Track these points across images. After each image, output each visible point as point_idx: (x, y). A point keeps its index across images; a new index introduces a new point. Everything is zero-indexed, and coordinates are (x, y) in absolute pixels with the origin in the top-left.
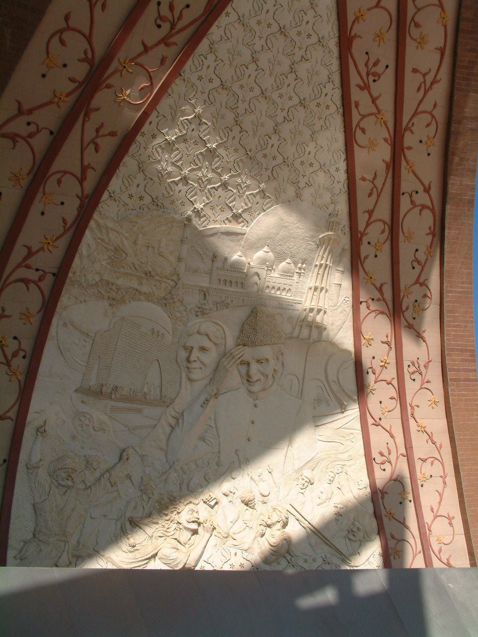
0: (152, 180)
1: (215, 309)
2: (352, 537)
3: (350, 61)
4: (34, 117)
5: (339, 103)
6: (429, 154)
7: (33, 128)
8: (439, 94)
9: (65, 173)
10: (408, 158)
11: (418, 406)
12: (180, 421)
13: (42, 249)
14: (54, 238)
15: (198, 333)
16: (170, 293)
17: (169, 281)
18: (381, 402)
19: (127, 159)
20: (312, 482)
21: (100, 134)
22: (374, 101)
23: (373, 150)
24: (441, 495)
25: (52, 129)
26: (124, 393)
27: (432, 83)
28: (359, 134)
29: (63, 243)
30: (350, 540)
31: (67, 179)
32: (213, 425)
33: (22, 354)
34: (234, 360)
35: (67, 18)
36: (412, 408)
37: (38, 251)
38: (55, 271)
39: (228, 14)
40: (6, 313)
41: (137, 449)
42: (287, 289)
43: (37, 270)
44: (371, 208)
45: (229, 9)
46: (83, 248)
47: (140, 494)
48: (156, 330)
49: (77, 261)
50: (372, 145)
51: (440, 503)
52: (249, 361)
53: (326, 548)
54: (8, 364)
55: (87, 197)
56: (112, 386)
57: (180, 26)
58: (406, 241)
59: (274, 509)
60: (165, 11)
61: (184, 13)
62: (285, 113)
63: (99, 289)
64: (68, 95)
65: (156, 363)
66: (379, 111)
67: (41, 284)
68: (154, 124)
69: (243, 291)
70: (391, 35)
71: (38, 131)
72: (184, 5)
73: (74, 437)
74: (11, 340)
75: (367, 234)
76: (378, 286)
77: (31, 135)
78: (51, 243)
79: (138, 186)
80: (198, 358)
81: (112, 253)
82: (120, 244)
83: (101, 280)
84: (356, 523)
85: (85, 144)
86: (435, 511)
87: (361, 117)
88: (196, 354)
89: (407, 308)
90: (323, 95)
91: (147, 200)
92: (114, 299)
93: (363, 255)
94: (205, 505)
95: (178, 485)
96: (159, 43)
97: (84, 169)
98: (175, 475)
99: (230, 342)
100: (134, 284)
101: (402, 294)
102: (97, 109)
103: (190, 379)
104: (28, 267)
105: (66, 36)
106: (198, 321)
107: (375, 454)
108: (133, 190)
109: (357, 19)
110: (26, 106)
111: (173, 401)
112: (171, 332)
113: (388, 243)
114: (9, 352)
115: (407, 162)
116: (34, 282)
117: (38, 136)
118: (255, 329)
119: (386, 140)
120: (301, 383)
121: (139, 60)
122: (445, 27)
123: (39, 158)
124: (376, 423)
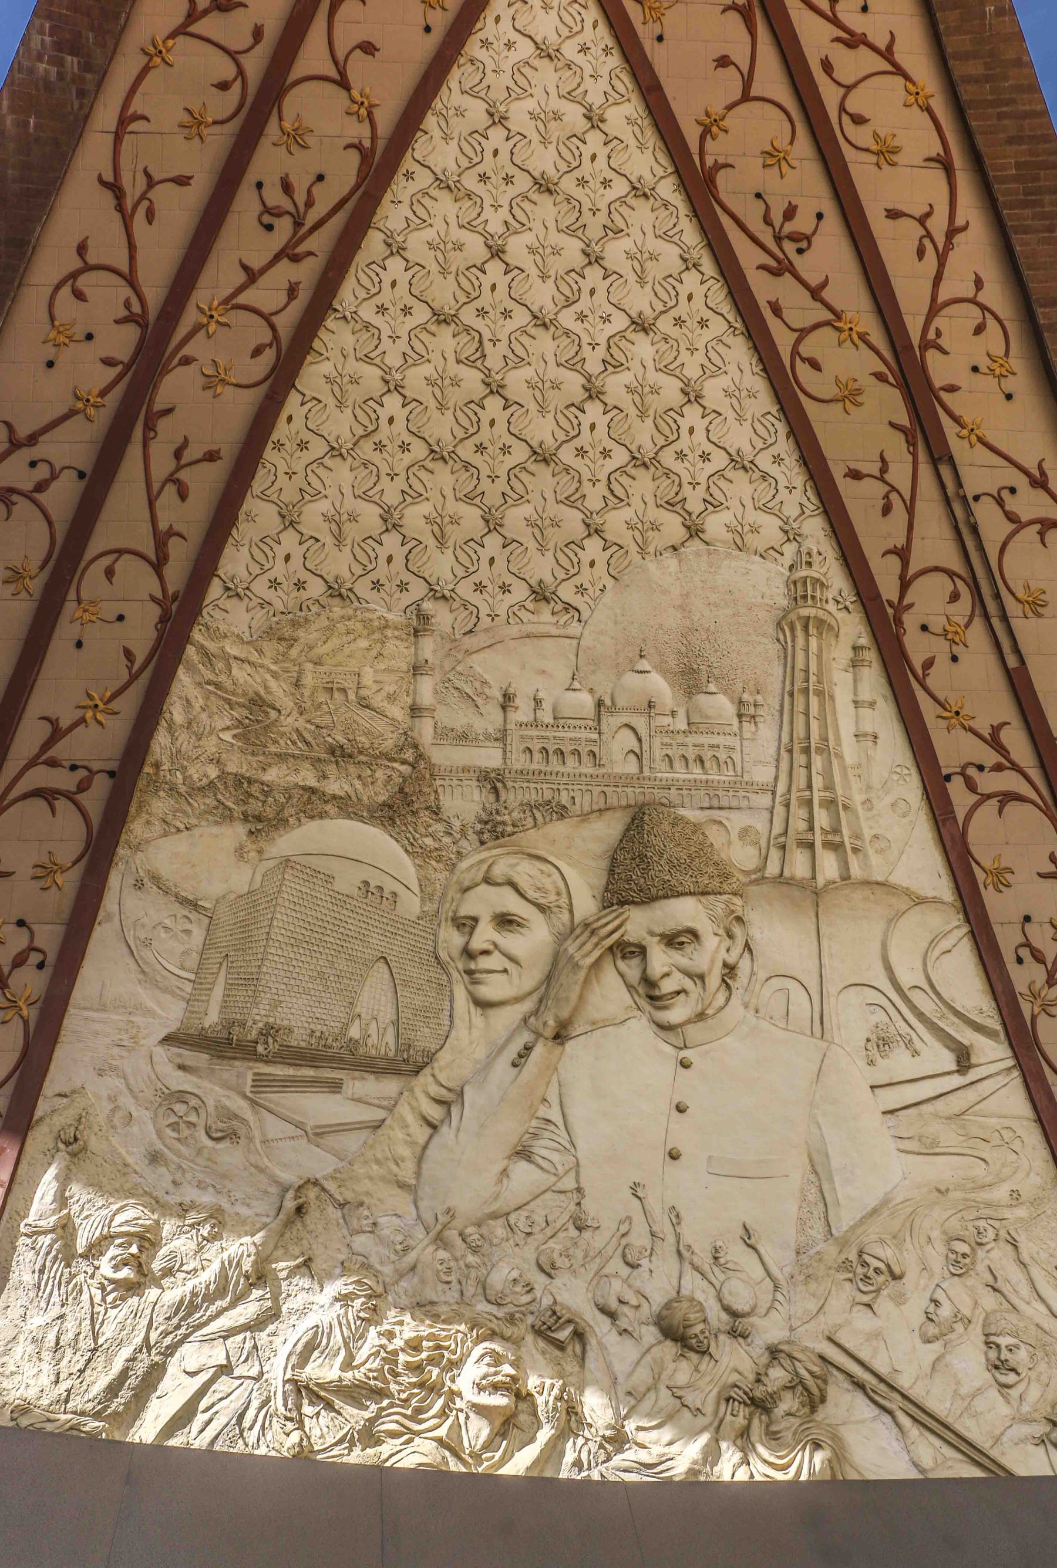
0: (317, 540)
1: (530, 822)
3: (725, 221)
4: (43, 449)
5: (726, 308)
6: (1009, 397)
8: (975, 255)
9: (120, 552)
10: (957, 412)
12: (455, 1111)
13: (83, 720)
14: (108, 694)
15: (488, 880)
16: (401, 790)
17: (396, 765)
19: (250, 504)
20: (897, 1270)
21: (183, 462)
22: (816, 293)
23: (859, 405)
26: (295, 1044)
27: (952, 232)
28: (803, 371)
29: (129, 704)
31: (126, 566)
33: (35, 958)
34: (594, 939)
35: (82, 249)
38: (113, 765)
39: (409, 176)
41: (331, 1186)
43: (74, 768)
44: (901, 542)
45: (408, 163)
46: (176, 711)
48: (373, 884)
49: (161, 739)
50: (849, 396)
52: (644, 943)
55: (175, 597)
56: (260, 1025)
57: (312, 217)
58: (1030, 614)
59: (774, 1352)
60: (275, 197)
61: (315, 190)
63: (220, 797)
64: (103, 394)
65: (381, 965)
66: (838, 316)
67: (83, 798)
68: (298, 422)
70: (803, 147)
71: (54, 476)
72: (313, 178)
73: (155, 1158)
74: (12, 928)
75: (910, 606)
76: (986, 732)
77: (41, 487)
78: (101, 706)
79: (287, 558)
80: (496, 945)
81: (245, 713)
82: (262, 692)
83: (223, 775)
85: (156, 487)
87: (796, 335)
88: (485, 935)
90: (683, 298)
91: (316, 588)
92: (259, 819)
94: (542, 1344)
95: (455, 1286)
96: (277, 258)
97: (161, 540)
98: (442, 1254)
99: (586, 905)
100: (308, 777)
102: (169, 411)
103: (483, 1005)
104: (53, 763)
105: (82, 282)
106: (484, 855)
108: (279, 570)
110: (23, 431)
111: (430, 1058)
112: (416, 889)
115: (957, 420)
116: (68, 796)
118: (642, 857)
119: (880, 377)
121: (241, 299)
122: (929, 110)
123: (61, 530)
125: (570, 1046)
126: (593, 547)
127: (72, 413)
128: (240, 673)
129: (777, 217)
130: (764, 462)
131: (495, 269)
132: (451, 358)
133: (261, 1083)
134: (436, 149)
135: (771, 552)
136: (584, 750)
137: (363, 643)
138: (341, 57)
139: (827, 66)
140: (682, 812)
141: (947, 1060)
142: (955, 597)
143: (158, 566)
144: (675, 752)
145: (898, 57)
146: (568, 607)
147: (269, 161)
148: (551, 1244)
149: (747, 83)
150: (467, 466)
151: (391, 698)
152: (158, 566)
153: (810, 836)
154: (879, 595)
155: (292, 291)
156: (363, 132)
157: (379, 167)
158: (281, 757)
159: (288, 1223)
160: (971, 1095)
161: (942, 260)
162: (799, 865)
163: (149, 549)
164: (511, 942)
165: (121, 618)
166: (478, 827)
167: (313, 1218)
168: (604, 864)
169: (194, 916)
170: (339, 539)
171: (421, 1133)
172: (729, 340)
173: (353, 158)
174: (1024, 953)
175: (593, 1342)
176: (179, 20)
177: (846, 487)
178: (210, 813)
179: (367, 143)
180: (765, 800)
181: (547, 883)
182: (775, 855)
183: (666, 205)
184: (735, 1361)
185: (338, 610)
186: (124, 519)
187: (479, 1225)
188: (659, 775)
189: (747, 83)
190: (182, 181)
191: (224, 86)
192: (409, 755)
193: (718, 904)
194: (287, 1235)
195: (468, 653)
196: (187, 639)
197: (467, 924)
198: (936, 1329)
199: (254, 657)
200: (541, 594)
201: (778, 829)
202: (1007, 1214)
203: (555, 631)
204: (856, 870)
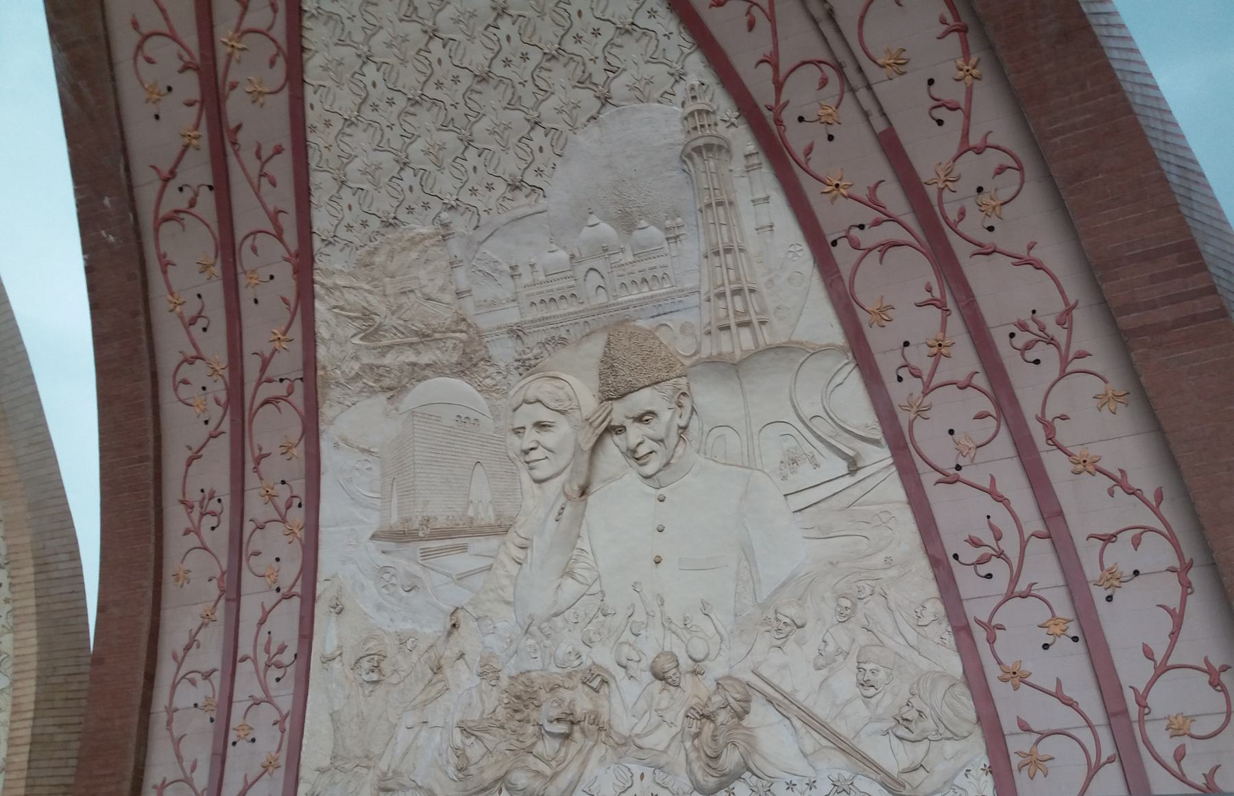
2: (902, 732)
7: (188, 194)
9: (254, 233)
13: (275, 350)
17: (458, 335)
18: (951, 432)
19: (316, 178)
24: (1178, 618)
25: (211, 183)
29: (296, 331)
30: (901, 739)
33: (296, 502)
36: (1049, 429)
40: (264, 452)
41: (470, 609)
42: (659, 274)
43: (281, 380)
46: (322, 331)
49: (321, 352)
51: (1174, 635)
67: (290, 398)
69: (581, 308)
71: (196, 195)
73: (379, 607)
77: (192, 204)
80: (538, 442)
81: (361, 322)
82: (365, 305)
84: (916, 702)
86: (1159, 657)
88: (531, 437)
91: (375, 224)
92: (390, 389)
95: (539, 659)
98: (531, 642)
103: (539, 482)
104: (270, 381)
106: (523, 382)
107: (952, 543)
108: (349, 218)
111: (513, 520)
117: (199, 199)
120: (744, 438)
124: (949, 479)
125: (591, 499)
133: (426, 554)
135: (666, 96)
136: (567, 294)
137: (414, 255)
140: (640, 323)
141: (842, 466)
143: (279, 236)
144: (627, 280)
148: (589, 627)
151: (442, 289)
152: (279, 236)
153: (726, 322)
154: (756, 106)
158: (390, 347)
159: (450, 634)
160: (856, 492)
162: (725, 344)
163: (269, 227)
164: (548, 438)
165: (272, 277)
166: (516, 364)
167: (463, 629)
168: (595, 372)
169: (370, 458)
171: (513, 569)
174: (904, 373)
178: (361, 391)
181: (561, 394)
182: (706, 341)
185: (391, 235)
187: (548, 620)
188: (620, 300)
192: (463, 326)
193: (667, 387)
194: (452, 640)
195: (480, 243)
196: (313, 282)
197: (518, 431)
198: (825, 662)
199: (356, 284)
200: (515, 187)
202: (882, 575)
203: (530, 211)
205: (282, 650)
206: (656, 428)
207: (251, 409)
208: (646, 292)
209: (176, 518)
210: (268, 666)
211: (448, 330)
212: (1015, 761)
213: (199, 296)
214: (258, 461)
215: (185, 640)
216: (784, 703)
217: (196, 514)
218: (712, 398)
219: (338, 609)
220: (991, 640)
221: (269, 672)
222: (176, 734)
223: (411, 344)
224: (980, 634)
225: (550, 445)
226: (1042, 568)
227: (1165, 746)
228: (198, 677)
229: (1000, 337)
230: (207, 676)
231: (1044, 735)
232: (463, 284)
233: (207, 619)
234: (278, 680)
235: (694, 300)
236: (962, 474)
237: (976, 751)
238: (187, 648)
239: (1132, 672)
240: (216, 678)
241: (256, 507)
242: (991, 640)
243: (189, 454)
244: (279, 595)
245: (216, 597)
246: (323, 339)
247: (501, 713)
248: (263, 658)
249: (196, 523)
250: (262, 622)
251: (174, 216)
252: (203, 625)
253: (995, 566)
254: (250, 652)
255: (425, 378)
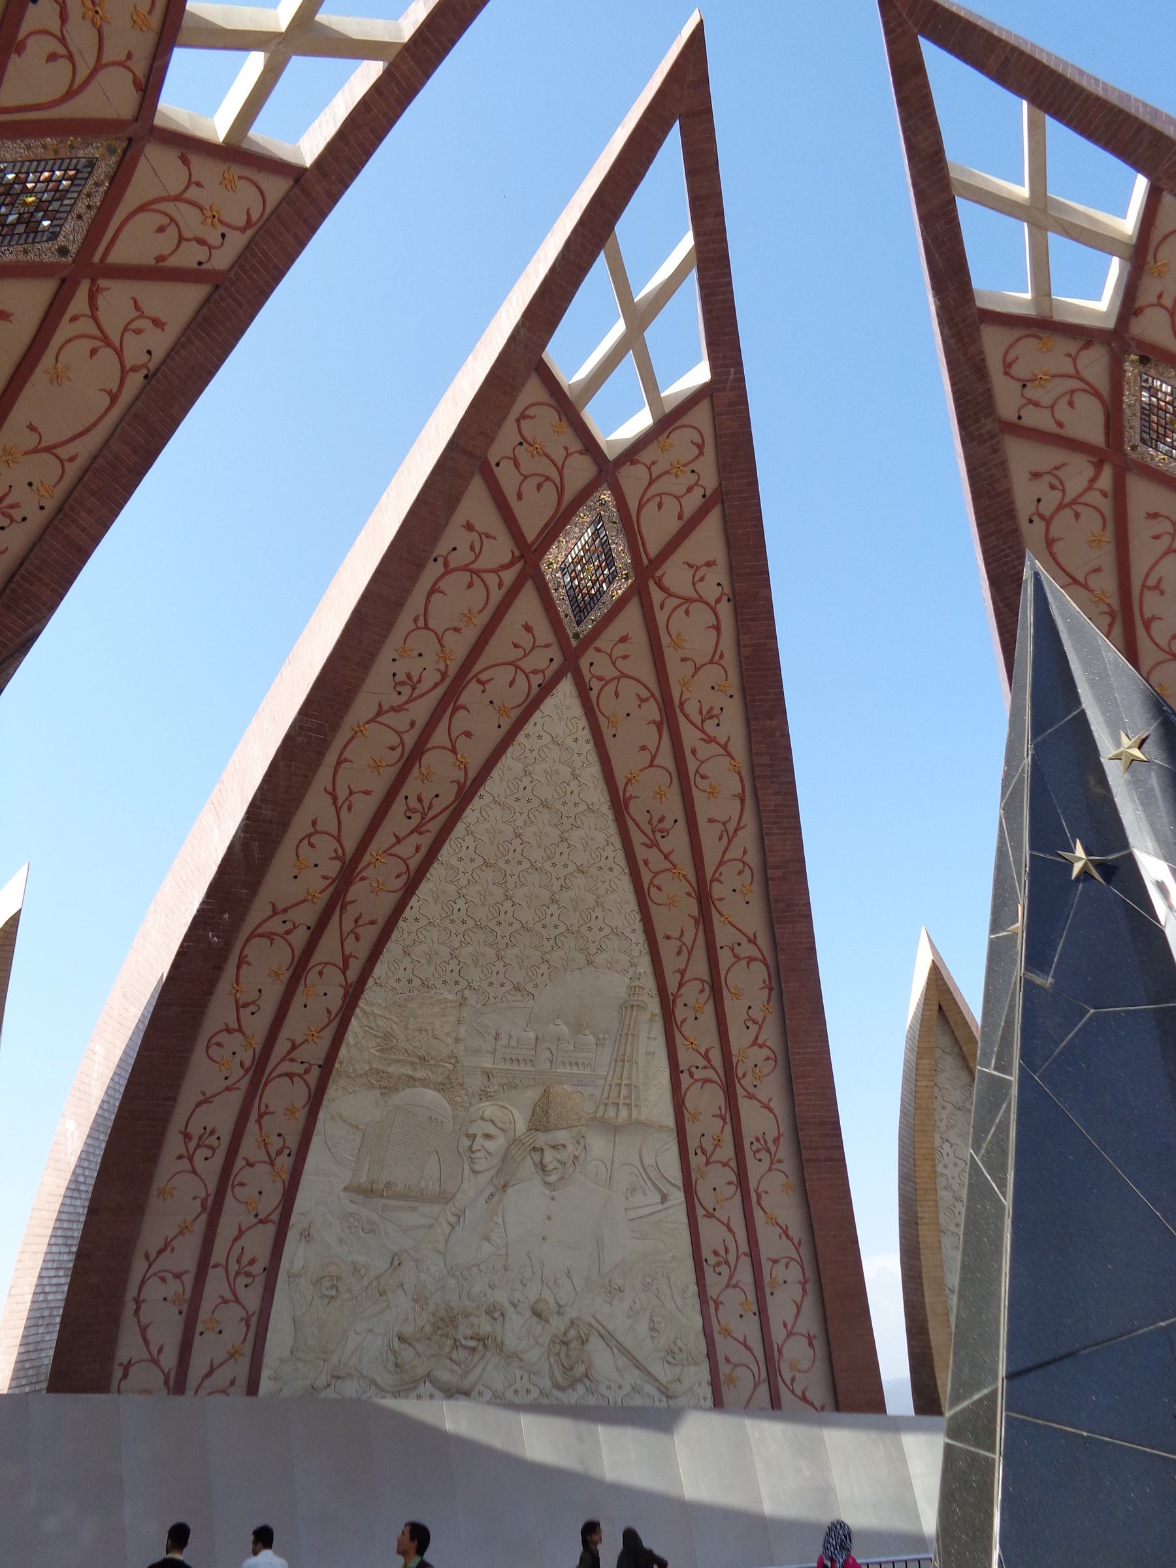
2: (670, 1359)
5: (623, 863)
7: (289, 926)
8: (747, 838)
9: (326, 964)
11: (766, 1192)
13: (307, 1041)
15: (482, 1119)
19: (390, 945)
22: (666, 857)
27: (736, 831)
28: (653, 890)
29: (328, 1034)
31: (328, 970)
32: (500, 1221)
33: (286, 1152)
35: (314, 823)
36: (759, 1196)
37: (302, 1044)
38: (321, 1063)
39: (481, 797)
40: (270, 1110)
41: (412, 1253)
44: (682, 967)
45: (481, 792)
46: (350, 1037)
47: (412, 1304)
49: (343, 1051)
53: (637, 1372)
54: (272, 1163)
57: (431, 814)
62: (561, 881)
66: (675, 867)
67: (306, 1077)
68: (415, 909)
71: (295, 927)
73: (341, 1241)
76: (703, 1051)
77: (288, 932)
84: (679, 1343)
85: (345, 935)
89: (744, 1075)
90: (603, 859)
93: (679, 1020)
96: (411, 833)
98: (454, 1281)
99: (521, 1127)
101: (735, 1060)
103: (474, 1172)
104: (292, 1060)
105: (314, 839)
107: (706, 1253)
108: (400, 974)
109: (629, 780)
110: (280, 907)
113: (711, 1002)
114: (273, 1150)
119: (689, 894)
122: (739, 773)
123: (298, 954)
125: (509, 1191)
126: (544, 968)
127: (305, 901)
128: (380, 1022)
129: (655, 821)
130: (628, 933)
131: (517, 842)
132: (490, 882)
134: (495, 785)
138: (454, 738)
139: (694, 752)
141: (658, 1198)
142: (702, 991)
145: (730, 748)
146: (529, 993)
147: (412, 787)
149: (653, 759)
150: (492, 931)
151: (447, 1034)
153: (617, 1101)
155: (418, 849)
156: (460, 775)
157: (467, 793)
158: (397, 1061)
161: (730, 841)
164: (490, 1145)
168: (531, 1110)
170: (429, 961)
171: (447, 1229)
172: (621, 877)
173: (455, 787)
174: (699, 1151)
175: (507, 1318)
176: (373, 714)
177: (663, 944)
179: (462, 780)
180: (602, 1082)
182: (602, 1108)
183: (603, 815)
184: (558, 1324)
186: (329, 947)
189: (653, 759)
190: (367, 793)
191: (393, 749)
193: (574, 1130)
199: (388, 1015)
200: (517, 988)
201: (605, 1095)
204: (635, 1115)
205: (252, 1262)
206: (564, 1155)
207: (270, 1074)
208: (575, 1070)
209: (173, 1144)
210: (238, 1273)
211: (442, 1060)
212: (722, 1379)
213: (260, 991)
214: (261, 1116)
215: (161, 1245)
216: (607, 1337)
217: (192, 1145)
218: (598, 1145)
219: (306, 1235)
220: (716, 1310)
221: (239, 1278)
222: (143, 1321)
223: (412, 1063)
224: (712, 1305)
225: (490, 1150)
226: (745, 1275)
227: (787, 1376)
228: (169, 1276)
229: (746, 1142)
230: (178, 1276)
231: (736, 1366)
232: (462, 1034)
233: (183, 1230)
234: (246, 1286)
235: (602, 1082)
236: (716, 1214)
237: (703, 1372)
238: (160, 1252)
239: (778, 1334)
240: (189, 1280)
241: (249, 1147)
242: (716, 1310)
243: (202, 1097)
244: (256, 1220)
245: (196, 1214)
246: (348, 1044)
247: (428, 1329)
248: (233, 1267)
249: (191, 1152)
250: (236, 1239)
251: (270, 936)
252: (181, 1233)
253: (724, 1269)
254: (223, 1261)
255: (414, 1086)
